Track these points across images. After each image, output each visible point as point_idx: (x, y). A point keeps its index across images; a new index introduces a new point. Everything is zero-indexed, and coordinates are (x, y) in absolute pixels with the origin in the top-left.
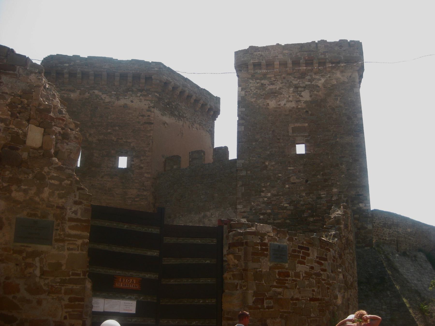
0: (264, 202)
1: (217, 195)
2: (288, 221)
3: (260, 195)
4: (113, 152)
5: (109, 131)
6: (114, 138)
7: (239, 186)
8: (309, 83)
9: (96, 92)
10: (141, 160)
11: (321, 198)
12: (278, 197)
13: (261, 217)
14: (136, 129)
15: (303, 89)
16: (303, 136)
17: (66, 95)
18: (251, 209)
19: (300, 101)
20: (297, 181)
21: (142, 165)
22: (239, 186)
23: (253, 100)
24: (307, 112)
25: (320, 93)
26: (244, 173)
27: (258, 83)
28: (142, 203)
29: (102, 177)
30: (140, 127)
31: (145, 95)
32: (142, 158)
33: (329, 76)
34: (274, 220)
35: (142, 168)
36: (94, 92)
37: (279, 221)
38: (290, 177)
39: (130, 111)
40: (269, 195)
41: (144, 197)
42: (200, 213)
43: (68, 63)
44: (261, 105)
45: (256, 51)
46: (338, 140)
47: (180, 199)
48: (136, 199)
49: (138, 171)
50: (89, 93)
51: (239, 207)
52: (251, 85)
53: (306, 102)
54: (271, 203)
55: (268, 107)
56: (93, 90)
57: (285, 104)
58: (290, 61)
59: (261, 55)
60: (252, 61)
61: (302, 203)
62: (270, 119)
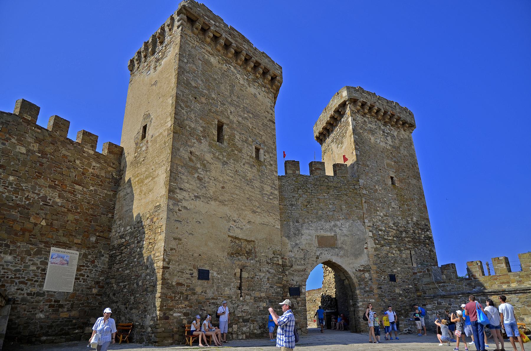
0: (380, 220)
1: (345, 207)
2: (395, 239)
3: (377, 214)
4: (250, 139)
5: (246, 115)
6: (249, 125)
7: (363, 202)
8: (389, 131)
9: (232, 68)
10: (271, 157)
11: (409, 224)
12: (387, 218)
13: (380, 233)
14: (264, 123)
15: (387, 135)
16: (393, 172)
17: (206, 56)
18: (373, 225)
19: (387, 143)
20: (395, 206)
21: (272, 162)
22: (363, 202)
23: (361, 131)
24: (391, 153)
25: (396, 141)
26: (364, 192)
27: (362, 119)
28: (275, 202)
29: (244, 164)
30: (267, 122)
31: (267, 93)
32: (271, 155)
33: (398, 130)
34: (388, 237)
35: (271, 165)
36: (230, 67)
37: (390, 238)
38: (391, 203)
39: (258, 102)
40: (382, 214)
41: (275, 196)
42: (329, 221)
43: (215, 22)
44: (367, 137)
45: (363, 92)
46: (410, 180)
47: (307, 205)
48: (271, 197)
49: (269, 167)
50: (226, 66)
51: (366, 221)
52: (358, 118)
53: (390, 145)
54: (384, 222)
55: (371, 141)
56: (229, 64)
57: (380, 143)
58: (383, 111)
59: (367, 97)
60: (362, 99)
61: (400, 225)
62: (373, 151)
